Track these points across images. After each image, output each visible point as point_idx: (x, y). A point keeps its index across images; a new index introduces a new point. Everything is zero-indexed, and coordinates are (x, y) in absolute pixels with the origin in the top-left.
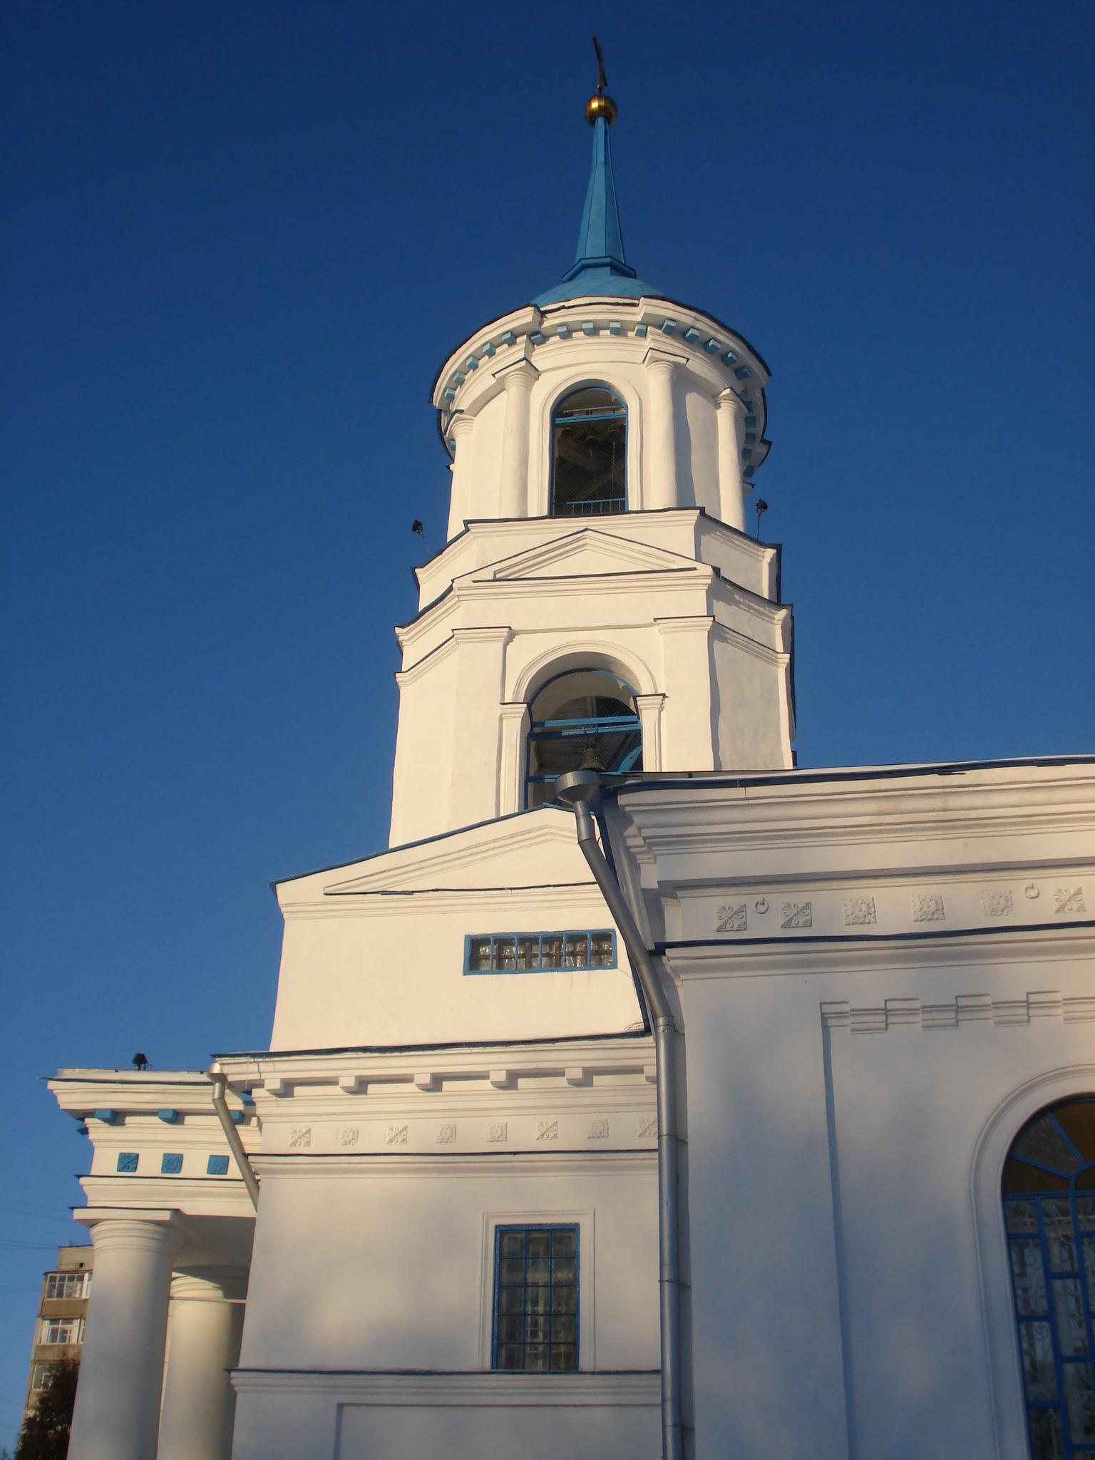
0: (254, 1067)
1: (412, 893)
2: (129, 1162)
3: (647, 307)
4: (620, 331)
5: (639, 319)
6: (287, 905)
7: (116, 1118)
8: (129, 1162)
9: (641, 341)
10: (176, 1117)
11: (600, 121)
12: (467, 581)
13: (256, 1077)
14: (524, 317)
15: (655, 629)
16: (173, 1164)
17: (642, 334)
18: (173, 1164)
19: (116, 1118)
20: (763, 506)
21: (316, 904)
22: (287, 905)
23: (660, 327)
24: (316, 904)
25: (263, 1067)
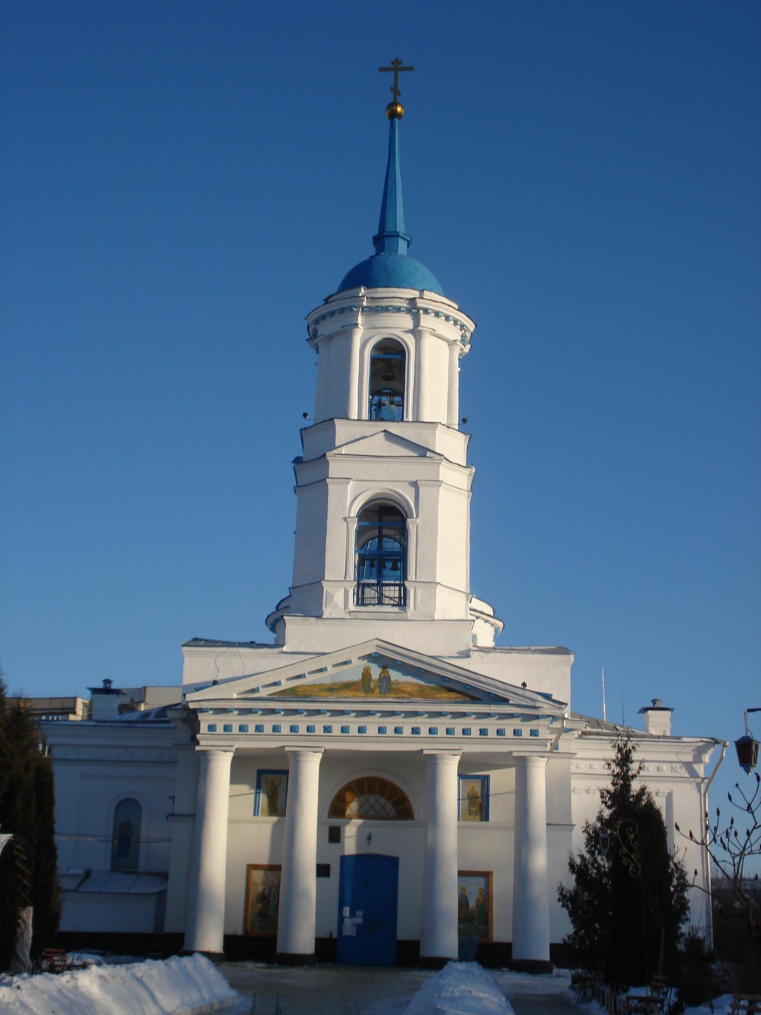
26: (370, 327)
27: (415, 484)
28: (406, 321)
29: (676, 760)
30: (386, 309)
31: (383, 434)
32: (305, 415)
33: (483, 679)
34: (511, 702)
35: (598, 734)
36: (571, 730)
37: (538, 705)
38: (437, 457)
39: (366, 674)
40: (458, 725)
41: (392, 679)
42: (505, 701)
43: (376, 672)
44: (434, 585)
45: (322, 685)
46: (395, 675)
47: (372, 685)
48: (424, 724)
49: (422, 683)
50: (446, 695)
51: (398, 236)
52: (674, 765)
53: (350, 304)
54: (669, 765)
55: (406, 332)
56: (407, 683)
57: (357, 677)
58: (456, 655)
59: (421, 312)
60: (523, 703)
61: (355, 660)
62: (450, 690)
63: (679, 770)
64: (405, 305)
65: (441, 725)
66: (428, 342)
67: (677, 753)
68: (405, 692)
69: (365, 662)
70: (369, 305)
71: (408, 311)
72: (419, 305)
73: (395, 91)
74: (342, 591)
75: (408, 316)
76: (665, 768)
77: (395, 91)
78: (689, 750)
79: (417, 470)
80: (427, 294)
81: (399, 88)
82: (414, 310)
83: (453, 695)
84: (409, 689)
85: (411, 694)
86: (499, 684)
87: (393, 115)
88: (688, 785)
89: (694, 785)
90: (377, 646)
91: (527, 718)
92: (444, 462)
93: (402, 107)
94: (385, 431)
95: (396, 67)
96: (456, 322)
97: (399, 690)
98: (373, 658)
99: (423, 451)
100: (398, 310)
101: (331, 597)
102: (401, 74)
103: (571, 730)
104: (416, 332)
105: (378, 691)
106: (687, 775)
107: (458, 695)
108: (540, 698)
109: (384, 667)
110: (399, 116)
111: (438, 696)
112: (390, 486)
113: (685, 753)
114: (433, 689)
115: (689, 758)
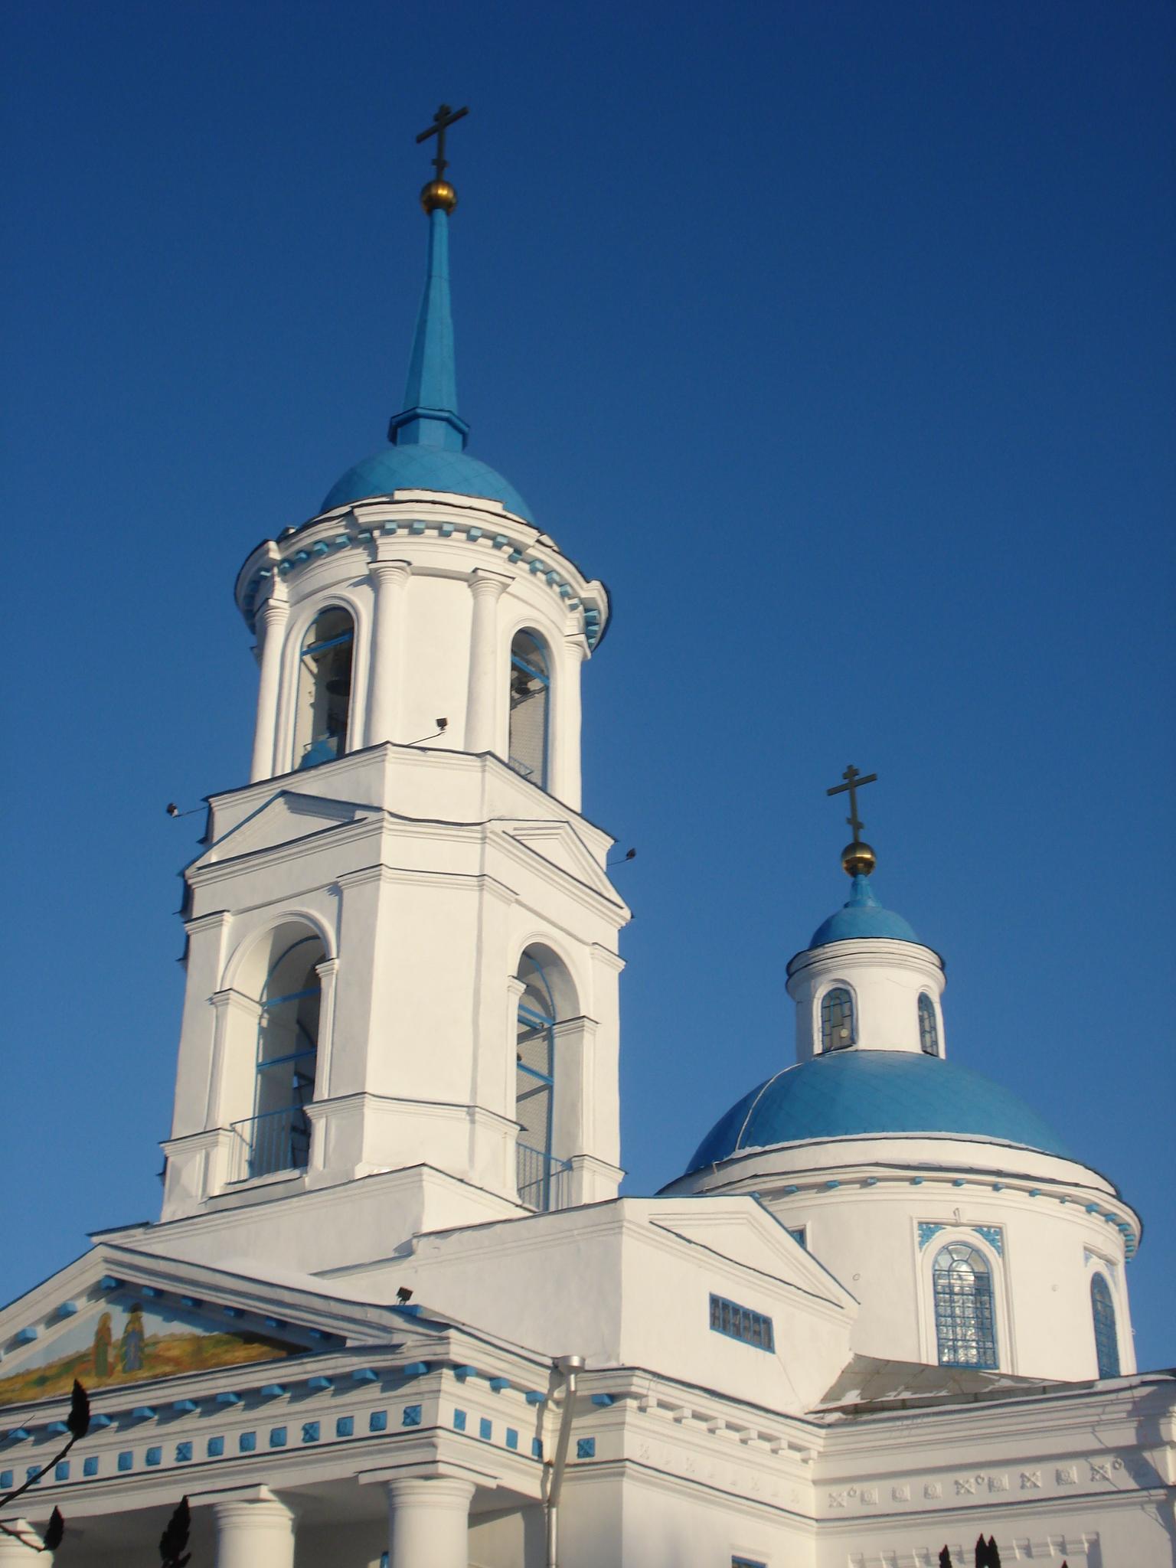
0: (646, 1383)
1: (689, 1241)
2: (460, 1418)
3: (593, 591)
4: (564, 595)
5: (583, 595)
6: (630, 1222)
7: (461, 1371)
8: (460, 1418)
9: (567, 611)
10: (497, 1384)
11: (440, 215)
12: (498, 826)
13: (644, 1391)
14: (527, 536)
15: (587, 949)
16: (486, 1427)
17: (573, 608)
18: (486, 1427)
19: (461, 1371)
20: (631, 854)
21: (643, 1228)
22: (630, 1222)
23: (586, 610)
24: (643, 1228)
25: (653, 1385)
26: (297, 600)
27: (336, 889)
28: (355, 562)
29: (1097, 1446)
30: (311, 555)
31: (281, 800)
32: (170, 810)
33: (287, 1297)
34: (349, 1344)
35: (904, 1405)
36: (613, 1398)
37: (397, 1339)
38: (372, 816)
39: (103, 1332)
40: (262, 1421)
41: (148, 1333)
42: (332, 1343)
43: (120, 1321)
44: (355, 1101)
45: (29, 1372)
46: (153, 1325)
47: (111, 1355)
48: (196, 1430)
49: (198, 1332)
50: (242, 1352)
51: (418, 416)
52: (1097, 1461)
53: (255, 569)
54: (1082, 1462)
55: (356, 585)
56: (174, 1338)
57: (85, 1342)
58: (392, 1255)
59: (376, 533)
60: (370, 1341)
61: (81, 1304)
62: (249, 1338)
63: (1110, 1474)
64: (342, 531)
65: (231, 1425)
66: (398, 590)
67: (1094, 1426)
68: (168, 1360)
69: (102, 1306)
70: (286, 554)
71: (353, 541)
72: (361, 520)
73: (440, 164)
74: (199, 1158)
75: (360, 550)
76: (1075, 1471)
77: (440, 164)
78: (1121, 1411)
79: (336, 857)
80: (399, 495)
81: (447, 156)
82: (365, 538)
83: (256, 1349)
84: (175, 1353)
85: (176, 1362)
86: (318, 1304)
87: (434, 204)
88: (1137, 1514)
89: (1152, 1509)
90: (107, 1261)
91: (395, 1378)
92: (389, 823)
93: (447, 184)
94: (284, 793)
95: (445, 118)
96: (492, 537)
97: (157, 1359)
98: (114, 1290)
99: (348, 815)
100: (333, 546)
101: (178, 1172)
102: (451, 130)
103: (613, 1398)
104: (373, 581)
105: (119, 1367)
106: (1133, 1485)
107: (265, 1349)
108: (398, 1322)
109: (135, 1309)
110: (446, 205)
111: (228, 1357)
112: (295, 906)
113: (1113, 1422)
114: (218, 1342)
115: (1127, 1436)
